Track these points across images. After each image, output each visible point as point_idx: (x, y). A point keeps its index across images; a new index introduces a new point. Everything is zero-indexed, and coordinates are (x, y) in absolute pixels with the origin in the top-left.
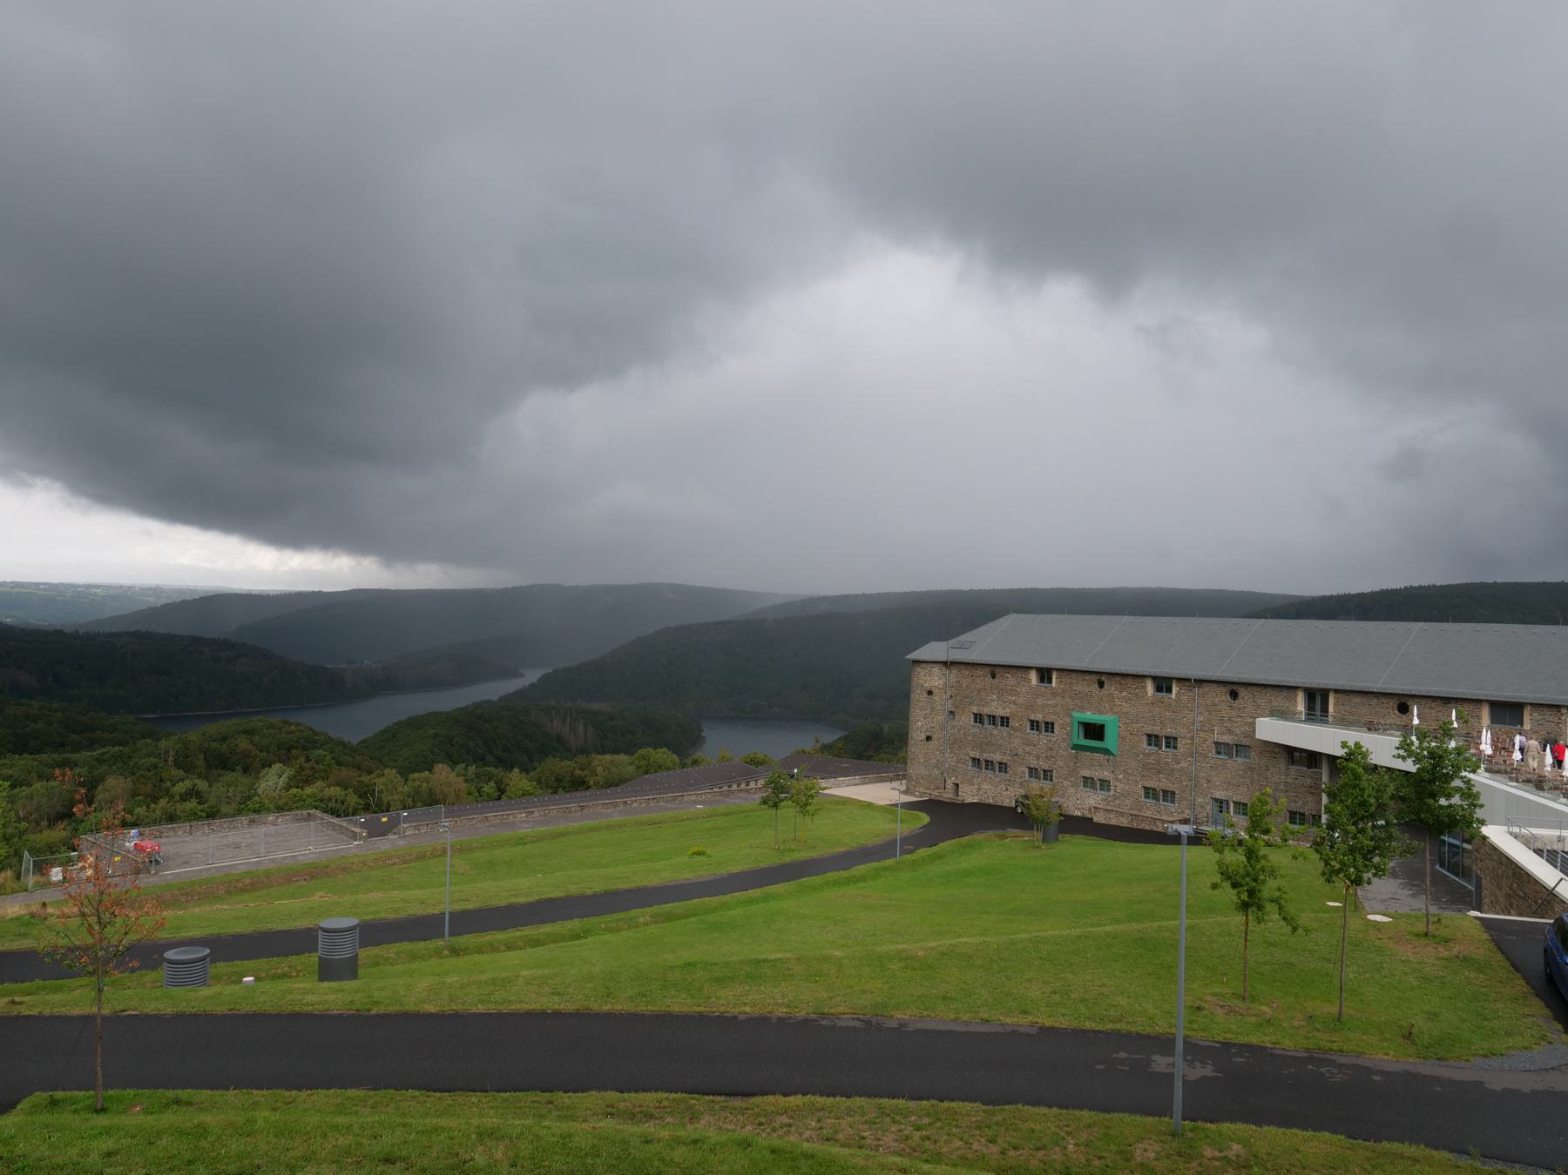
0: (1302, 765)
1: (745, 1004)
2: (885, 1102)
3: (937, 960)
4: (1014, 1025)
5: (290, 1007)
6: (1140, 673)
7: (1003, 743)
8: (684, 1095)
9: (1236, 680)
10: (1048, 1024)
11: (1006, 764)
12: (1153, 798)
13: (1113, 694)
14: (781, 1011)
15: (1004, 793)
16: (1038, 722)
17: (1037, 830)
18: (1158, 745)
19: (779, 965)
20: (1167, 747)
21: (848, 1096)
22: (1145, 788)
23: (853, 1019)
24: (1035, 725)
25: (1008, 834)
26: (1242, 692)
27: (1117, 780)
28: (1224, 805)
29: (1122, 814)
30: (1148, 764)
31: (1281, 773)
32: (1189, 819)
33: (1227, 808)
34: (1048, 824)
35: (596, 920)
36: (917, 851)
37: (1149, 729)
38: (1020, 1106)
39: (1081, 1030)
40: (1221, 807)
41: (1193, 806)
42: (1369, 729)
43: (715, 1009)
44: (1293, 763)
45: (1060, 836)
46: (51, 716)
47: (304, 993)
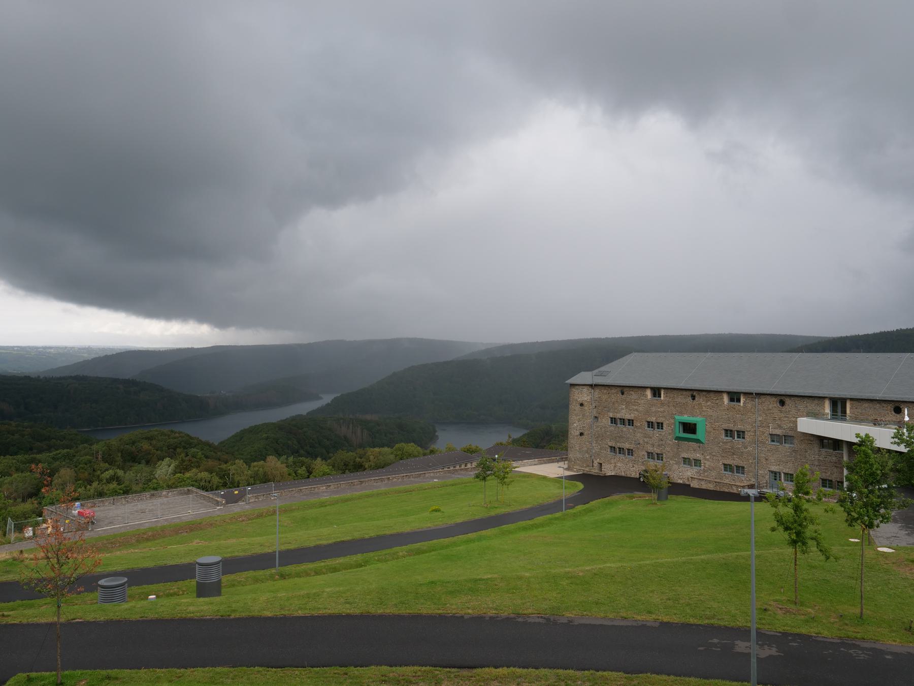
0: (829, 448)
1: (469, 608)
2: (561, 672)
3: (592, 578)
4: (643, 621)
5: (179, 615)
6: (719, 390)
7: (630, 437)
8: (431, 668)
9: (783, 393)
10: (666, 619)
11: (632, 450)
12: (730, 471)
13: (701, 404)
14: (492, 613)
15: (632, 469)
16: (652, 422)
17: (654, 492)
18: (732, 436)
19: (490, 582)
20: (738, 437)
21: (537, 668)
22: (724, 464)
23: (538, 617)
24: (650, 424)
25: (635, 496)
26: (787, 401)
27: (706, 459)
28: (778, 475)
29: (710, 482)
30: (726, 449)
31: (815, 453)
32: (754, 485)
33: (780, 477)
34: (661, 488)
35: (371, 554)
36: (576, 507)
37: (726, 426)
38: (649, 674)
39: (688, 624)
40: (776, 477)
41: (756, 476)
42: (875, 424)
43: (449, 612)
44: (823, 447)
45: (669, 496)
46: (24, 431)
47: (188, 606)
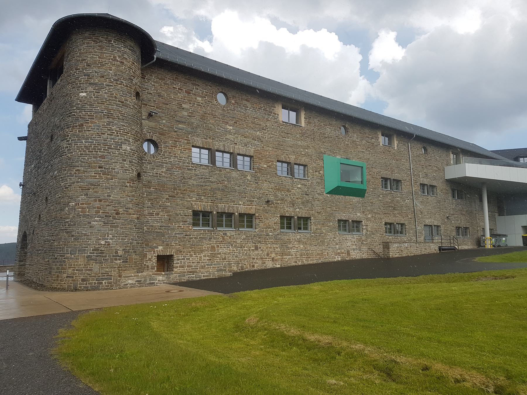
27: (368, 219)
